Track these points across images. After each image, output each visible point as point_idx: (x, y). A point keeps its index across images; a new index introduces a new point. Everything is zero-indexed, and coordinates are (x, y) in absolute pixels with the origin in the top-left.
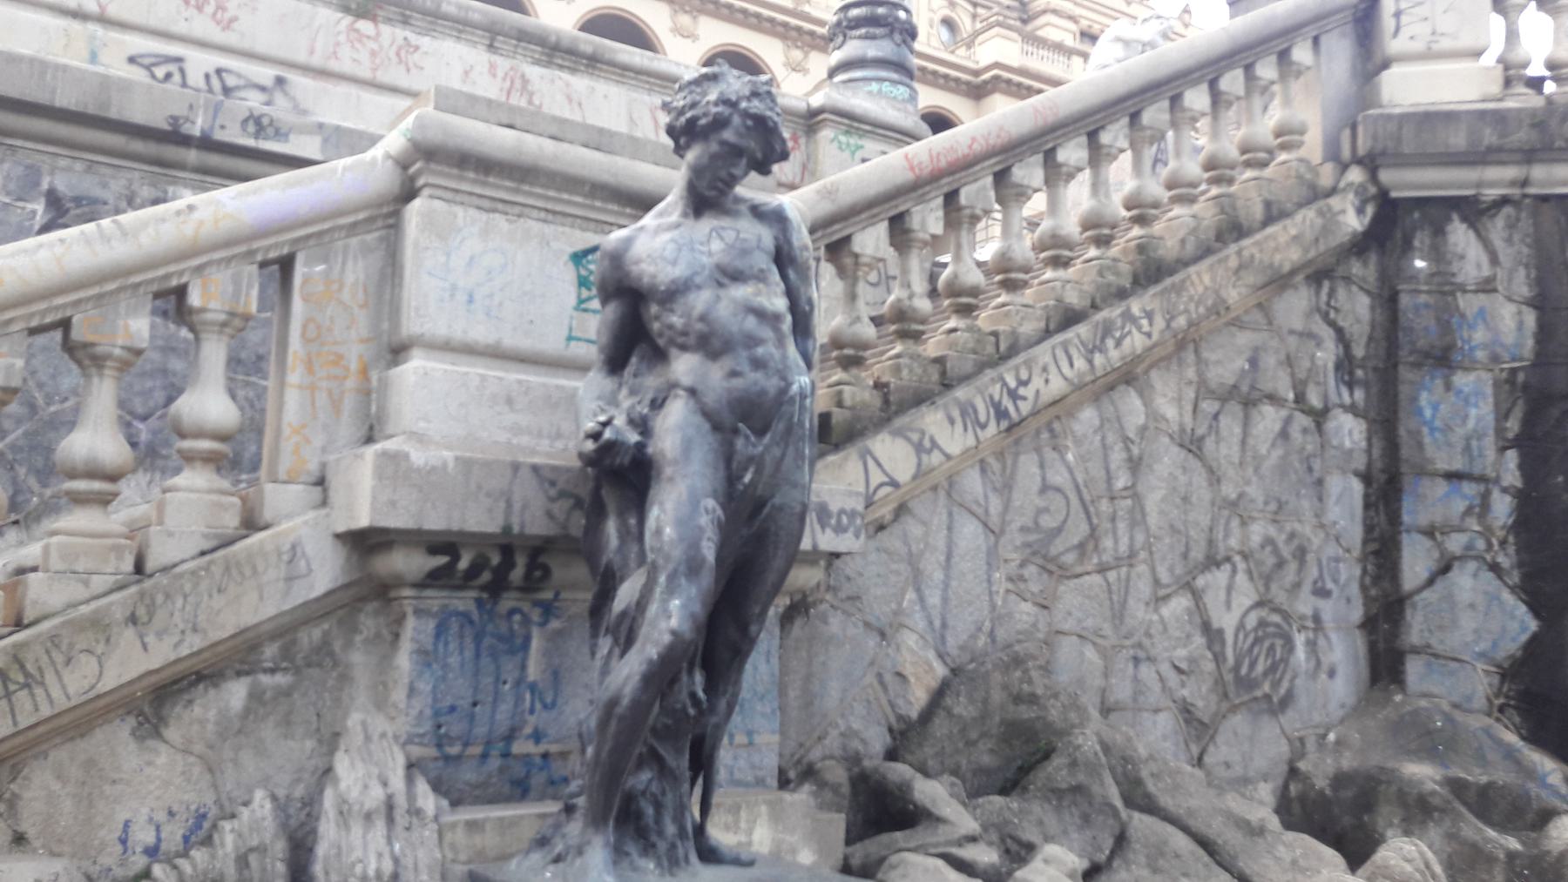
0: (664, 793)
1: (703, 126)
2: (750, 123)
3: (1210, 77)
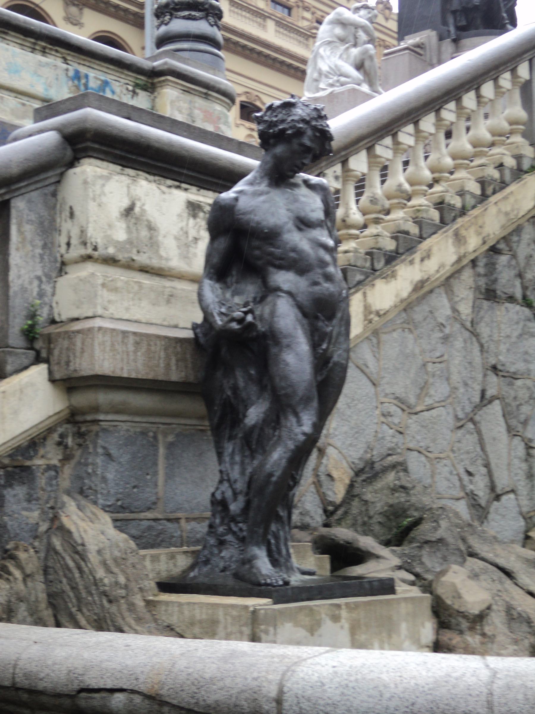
0: (278, 530)
1: (289, 134)
2: (318, 134)
3: (476, 87)
